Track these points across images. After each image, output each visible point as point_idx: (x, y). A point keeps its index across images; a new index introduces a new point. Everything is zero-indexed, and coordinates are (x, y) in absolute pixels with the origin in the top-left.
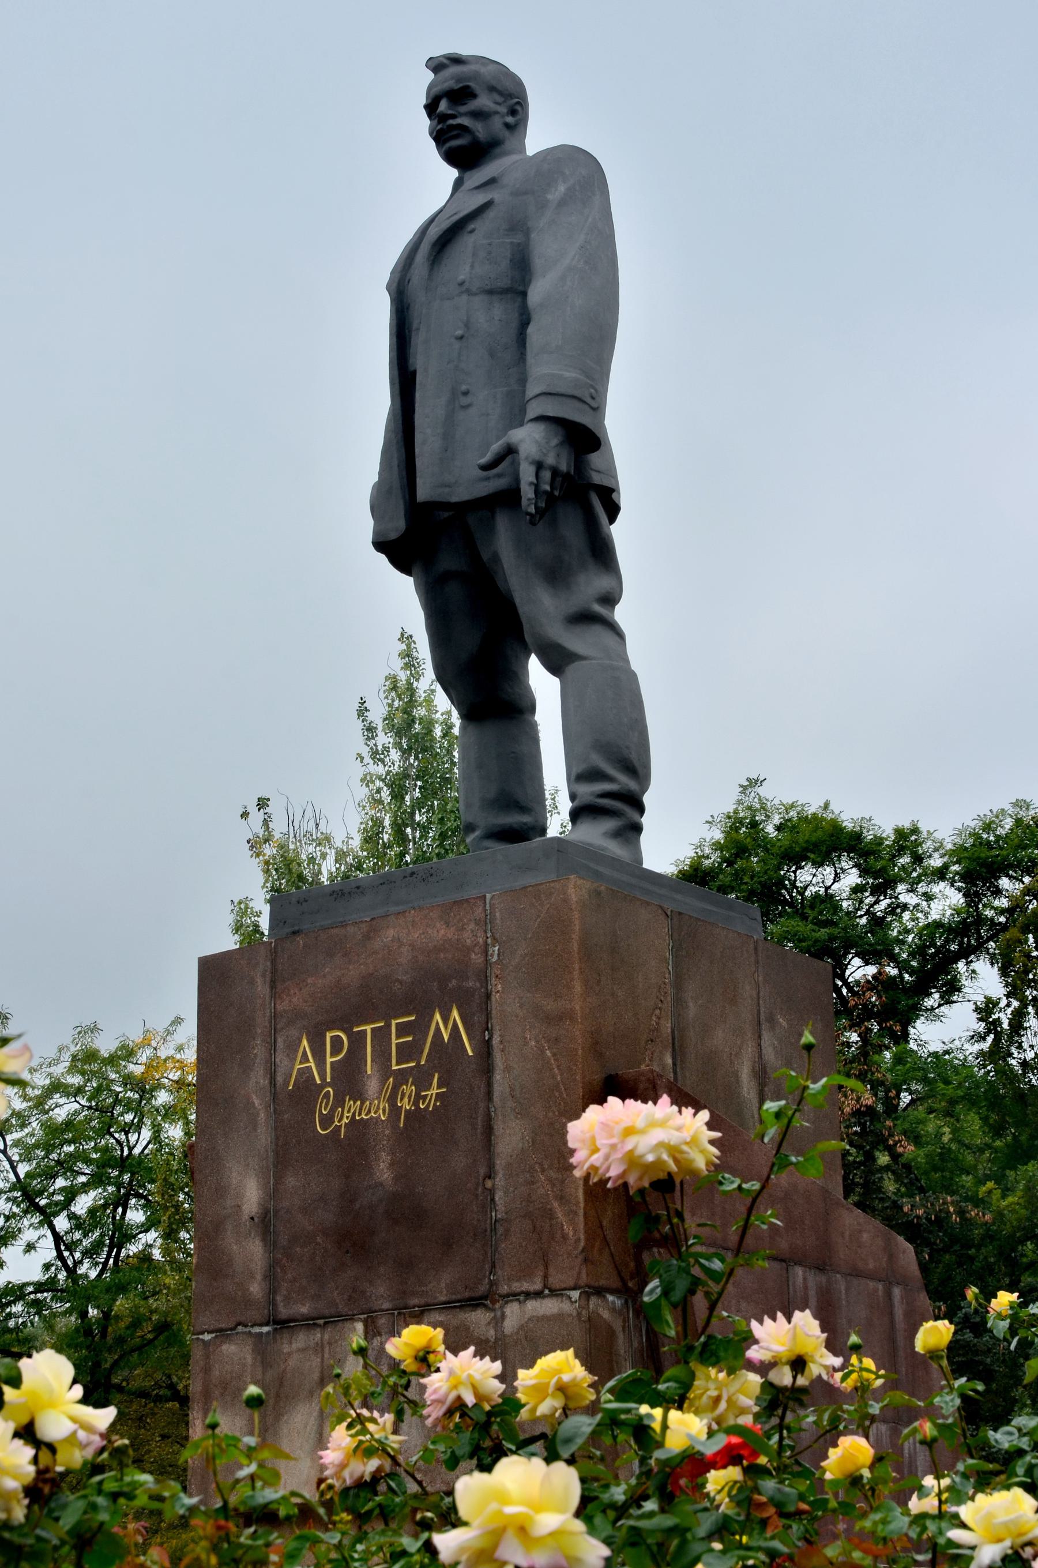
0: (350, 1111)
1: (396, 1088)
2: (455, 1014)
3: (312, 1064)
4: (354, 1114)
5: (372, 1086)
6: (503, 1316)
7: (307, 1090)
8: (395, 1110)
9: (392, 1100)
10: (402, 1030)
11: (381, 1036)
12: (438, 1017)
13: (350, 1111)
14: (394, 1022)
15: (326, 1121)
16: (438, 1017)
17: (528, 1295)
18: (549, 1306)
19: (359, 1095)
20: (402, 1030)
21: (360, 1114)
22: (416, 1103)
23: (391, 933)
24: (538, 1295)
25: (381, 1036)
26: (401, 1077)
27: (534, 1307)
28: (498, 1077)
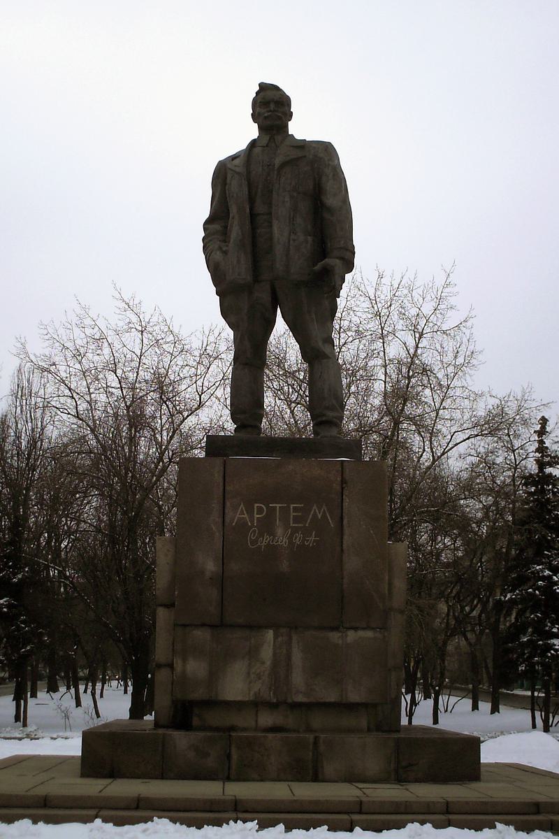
0: (266, 540)
1: (292, 534)
2: (324, 508)
3: (246, 516)
4: (269, 542)
5: (279, 531)
6: (346, 636)
7: (242, 528)
8: (291, 543)
9: (290, 538)
10: (295, 509)
11: (285, 511)
12: (315, 507)
13: (266, 540)
14: (292, 506)
15: (256, 541)
16: (315, 507)
18: (369, 634)
19: (272, 533)
20: (295, 509)
21: (272, 542)
22: (303, 541)
23: (291, 467)
24: (364, 629)
25: (285, 511)
26: (295, 530)
27: (361, 633)
28: (345, 537)
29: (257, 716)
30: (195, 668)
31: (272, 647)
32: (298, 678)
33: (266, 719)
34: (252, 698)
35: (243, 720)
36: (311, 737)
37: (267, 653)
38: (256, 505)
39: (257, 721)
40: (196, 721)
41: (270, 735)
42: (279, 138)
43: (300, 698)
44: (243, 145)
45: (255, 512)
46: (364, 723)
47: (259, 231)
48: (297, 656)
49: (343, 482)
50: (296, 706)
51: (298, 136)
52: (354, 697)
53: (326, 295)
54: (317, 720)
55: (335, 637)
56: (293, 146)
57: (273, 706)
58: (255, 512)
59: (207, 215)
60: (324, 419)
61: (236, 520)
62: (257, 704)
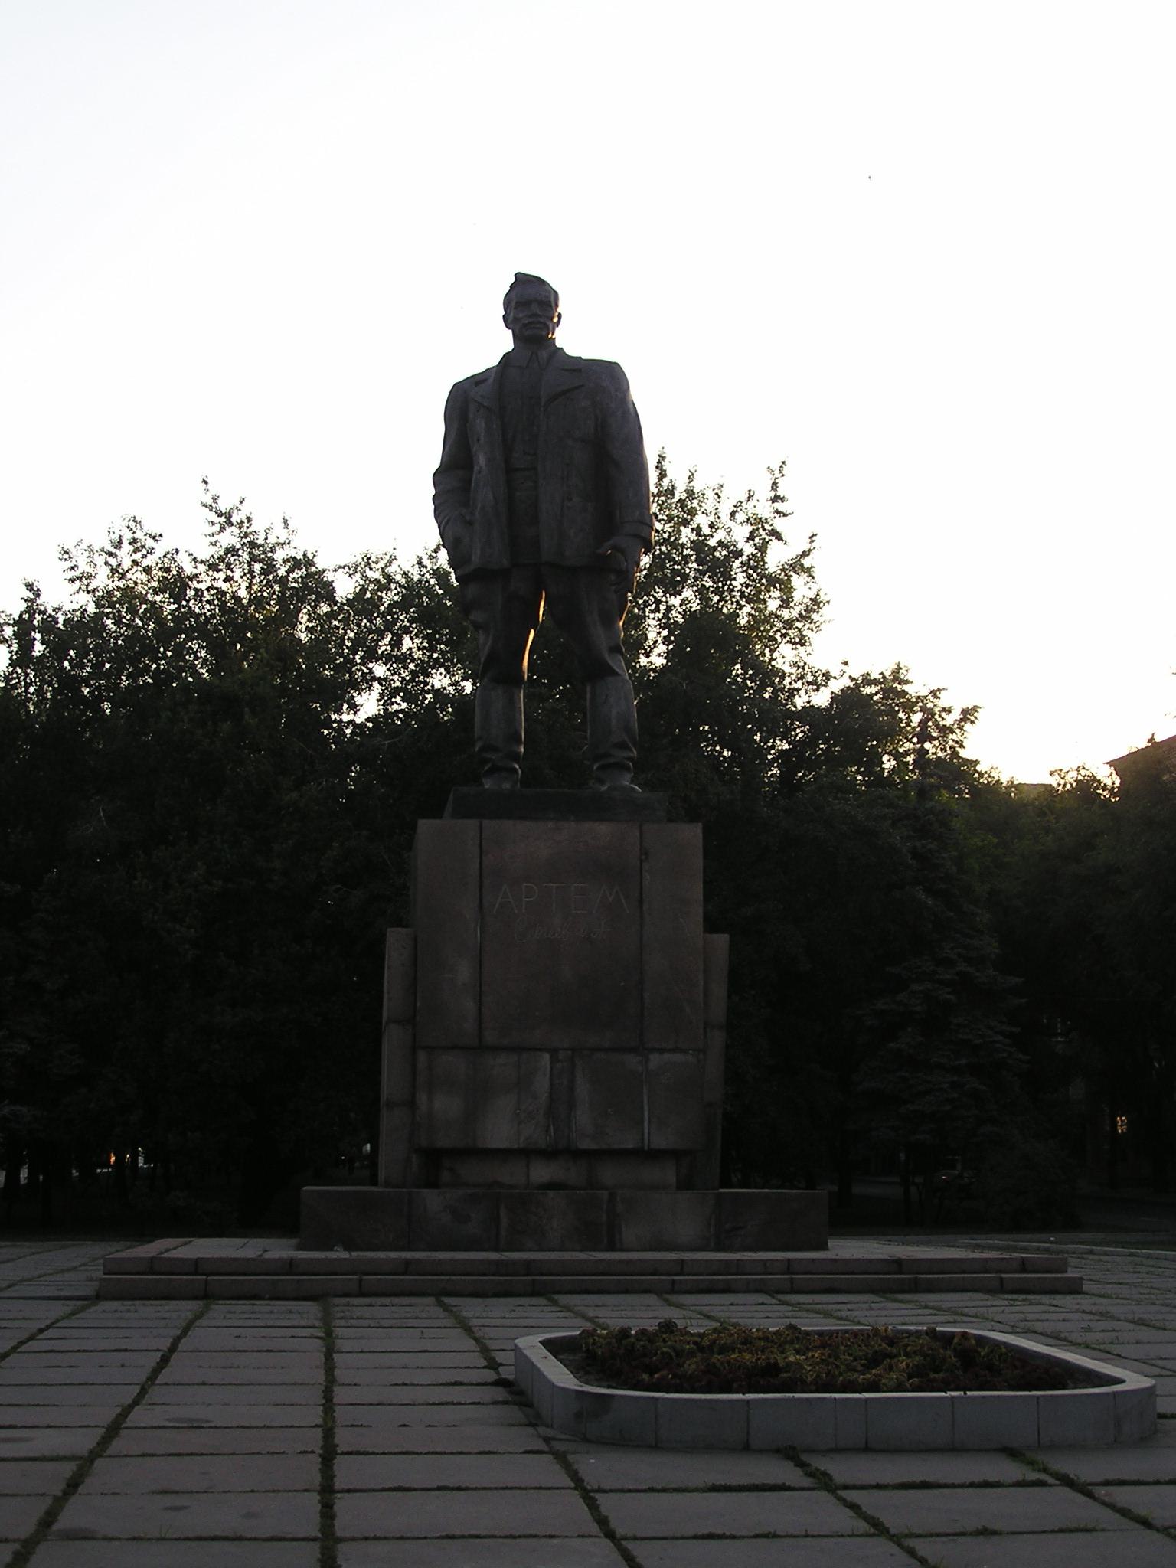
3: (511, 900)
17: (662, 1051)
18: (678, 1057)
27: (666, 1056)
29: (528, 1166)
30: (446, 1105)
31: (548, 1076)
32: (583, 1118)
33: (541, 1172)
34: (522, 1146)
35: (510, 1174)
36: (605, 1194)
37: (542, 1084)
38: (525, 884)
39: (528, 1176)
40: (446, 1176)
41: (551, 1193)
42: (544, 354)
43: (586, 1144)
44: (494, 361)
45: (524, 896)
46: (671, 1177)
47: (518, 494)
48: (583, 1089)
49: (645, 854)
50: (578, 1154)
51: (572, 351)
52: (660, 1142)
53: (613, 588)
54: (609, 1174)
55: (632, 1061)
56: (567, 370)
57: (549, 1154)
58: (524, 896)
59: (437, 464)
60: (612, 761)
61: (497, 906)
62: (527, 1153)
